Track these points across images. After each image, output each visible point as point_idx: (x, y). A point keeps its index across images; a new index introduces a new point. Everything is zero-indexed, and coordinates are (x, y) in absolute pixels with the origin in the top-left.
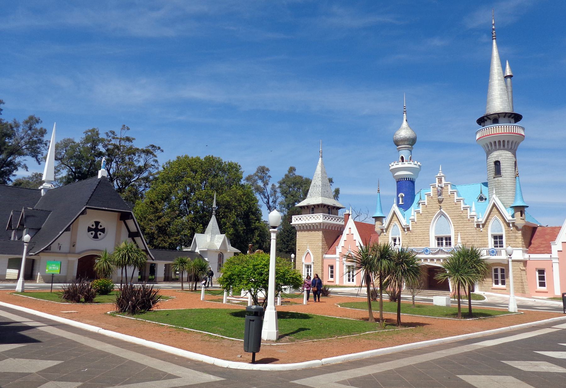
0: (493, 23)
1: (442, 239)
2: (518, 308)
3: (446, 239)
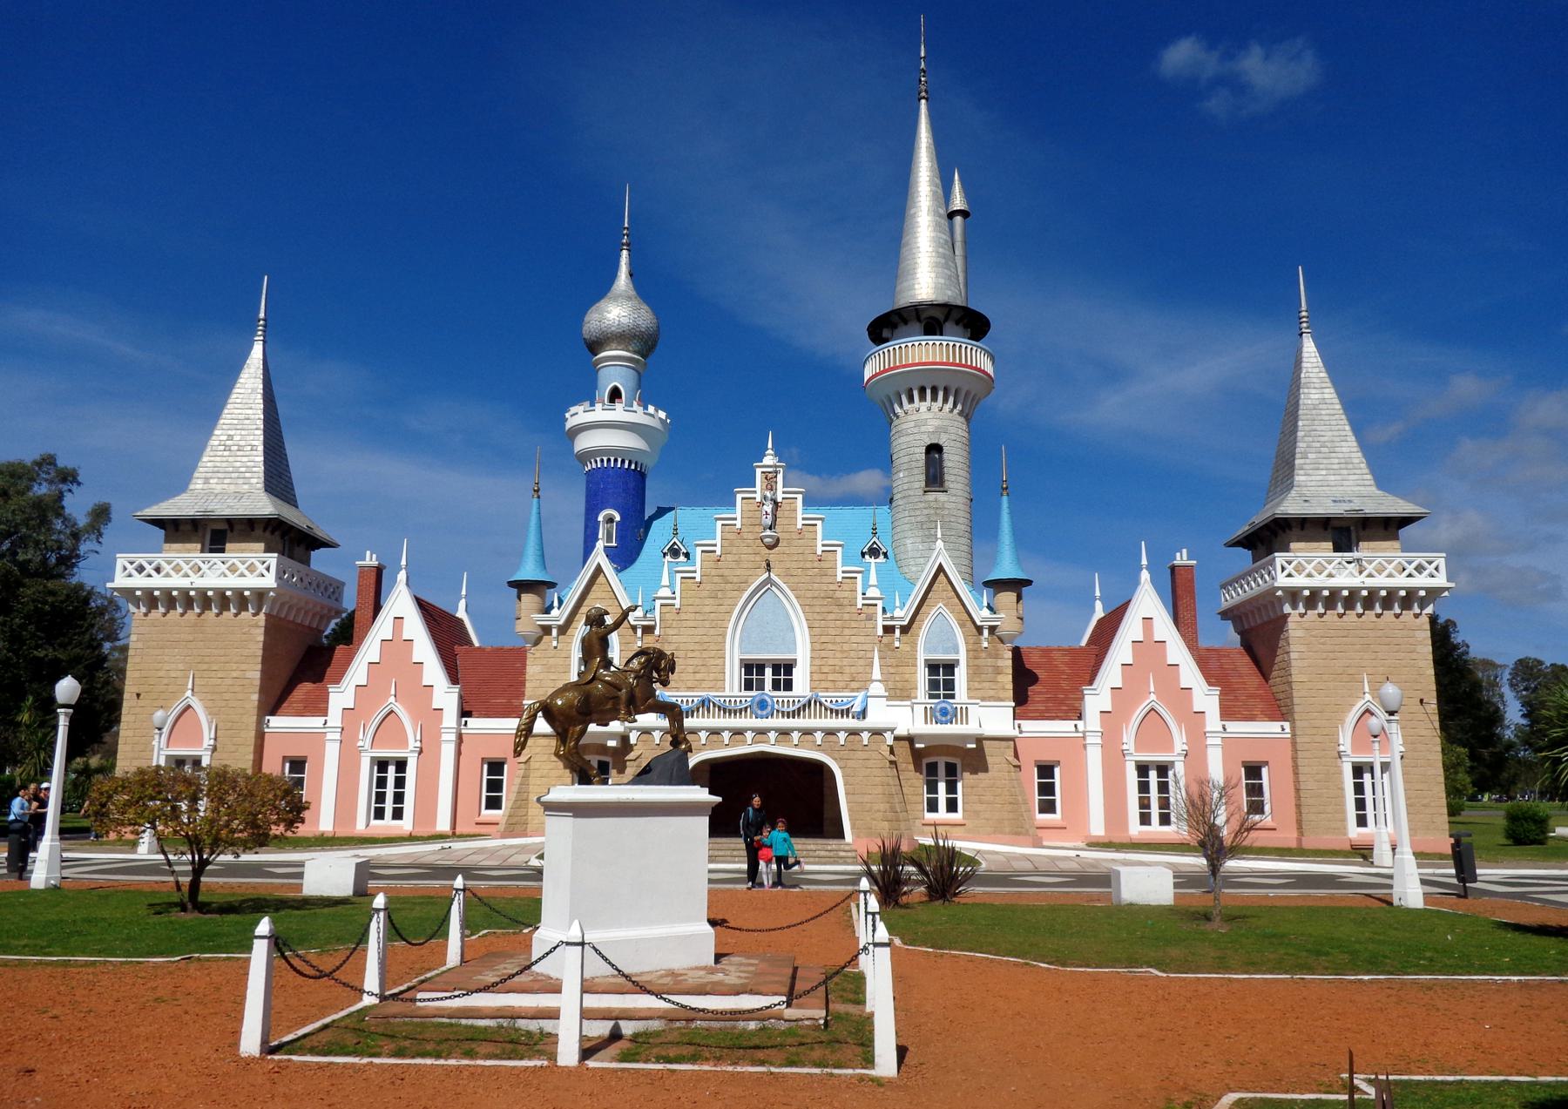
0: (923, 55)
1: (761, 668)
3: (776, 669)
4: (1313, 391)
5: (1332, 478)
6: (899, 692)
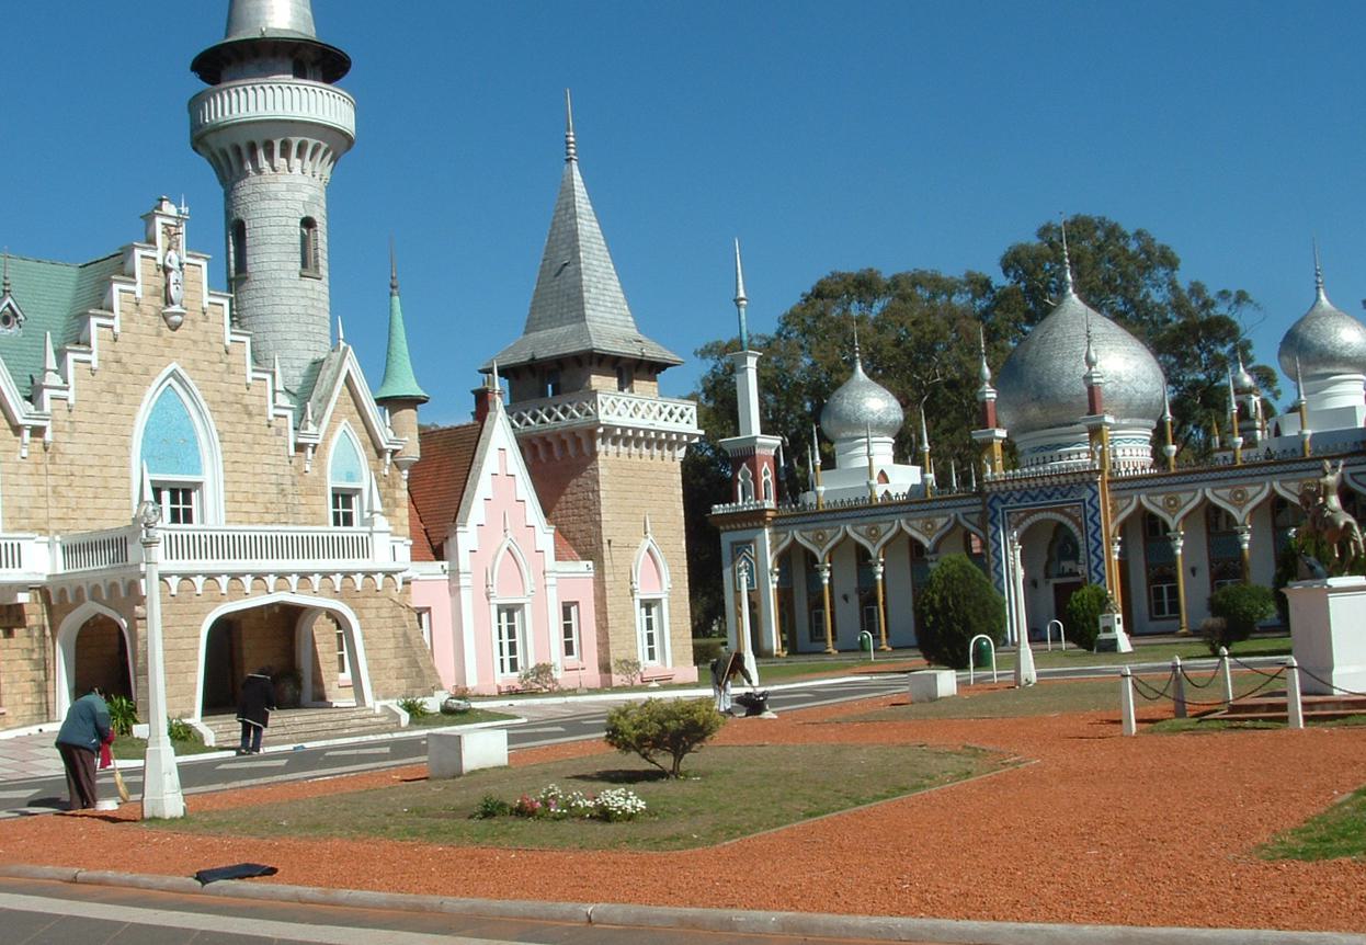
2: (176, 755)
4: (585, 222)
5: (607, 315)
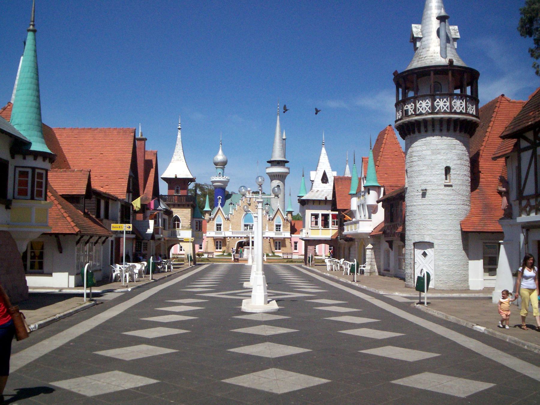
6: (271, 230)
